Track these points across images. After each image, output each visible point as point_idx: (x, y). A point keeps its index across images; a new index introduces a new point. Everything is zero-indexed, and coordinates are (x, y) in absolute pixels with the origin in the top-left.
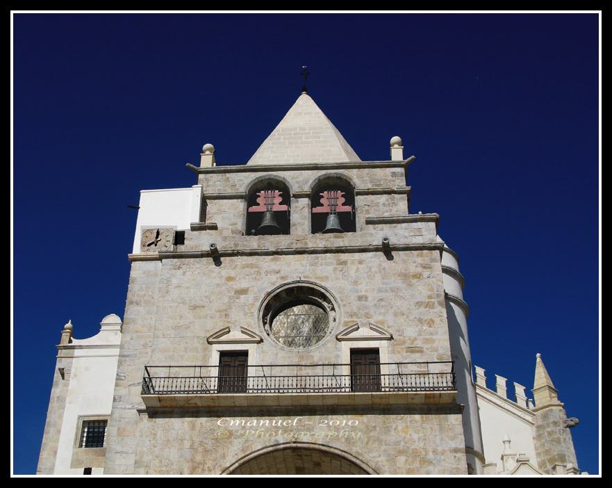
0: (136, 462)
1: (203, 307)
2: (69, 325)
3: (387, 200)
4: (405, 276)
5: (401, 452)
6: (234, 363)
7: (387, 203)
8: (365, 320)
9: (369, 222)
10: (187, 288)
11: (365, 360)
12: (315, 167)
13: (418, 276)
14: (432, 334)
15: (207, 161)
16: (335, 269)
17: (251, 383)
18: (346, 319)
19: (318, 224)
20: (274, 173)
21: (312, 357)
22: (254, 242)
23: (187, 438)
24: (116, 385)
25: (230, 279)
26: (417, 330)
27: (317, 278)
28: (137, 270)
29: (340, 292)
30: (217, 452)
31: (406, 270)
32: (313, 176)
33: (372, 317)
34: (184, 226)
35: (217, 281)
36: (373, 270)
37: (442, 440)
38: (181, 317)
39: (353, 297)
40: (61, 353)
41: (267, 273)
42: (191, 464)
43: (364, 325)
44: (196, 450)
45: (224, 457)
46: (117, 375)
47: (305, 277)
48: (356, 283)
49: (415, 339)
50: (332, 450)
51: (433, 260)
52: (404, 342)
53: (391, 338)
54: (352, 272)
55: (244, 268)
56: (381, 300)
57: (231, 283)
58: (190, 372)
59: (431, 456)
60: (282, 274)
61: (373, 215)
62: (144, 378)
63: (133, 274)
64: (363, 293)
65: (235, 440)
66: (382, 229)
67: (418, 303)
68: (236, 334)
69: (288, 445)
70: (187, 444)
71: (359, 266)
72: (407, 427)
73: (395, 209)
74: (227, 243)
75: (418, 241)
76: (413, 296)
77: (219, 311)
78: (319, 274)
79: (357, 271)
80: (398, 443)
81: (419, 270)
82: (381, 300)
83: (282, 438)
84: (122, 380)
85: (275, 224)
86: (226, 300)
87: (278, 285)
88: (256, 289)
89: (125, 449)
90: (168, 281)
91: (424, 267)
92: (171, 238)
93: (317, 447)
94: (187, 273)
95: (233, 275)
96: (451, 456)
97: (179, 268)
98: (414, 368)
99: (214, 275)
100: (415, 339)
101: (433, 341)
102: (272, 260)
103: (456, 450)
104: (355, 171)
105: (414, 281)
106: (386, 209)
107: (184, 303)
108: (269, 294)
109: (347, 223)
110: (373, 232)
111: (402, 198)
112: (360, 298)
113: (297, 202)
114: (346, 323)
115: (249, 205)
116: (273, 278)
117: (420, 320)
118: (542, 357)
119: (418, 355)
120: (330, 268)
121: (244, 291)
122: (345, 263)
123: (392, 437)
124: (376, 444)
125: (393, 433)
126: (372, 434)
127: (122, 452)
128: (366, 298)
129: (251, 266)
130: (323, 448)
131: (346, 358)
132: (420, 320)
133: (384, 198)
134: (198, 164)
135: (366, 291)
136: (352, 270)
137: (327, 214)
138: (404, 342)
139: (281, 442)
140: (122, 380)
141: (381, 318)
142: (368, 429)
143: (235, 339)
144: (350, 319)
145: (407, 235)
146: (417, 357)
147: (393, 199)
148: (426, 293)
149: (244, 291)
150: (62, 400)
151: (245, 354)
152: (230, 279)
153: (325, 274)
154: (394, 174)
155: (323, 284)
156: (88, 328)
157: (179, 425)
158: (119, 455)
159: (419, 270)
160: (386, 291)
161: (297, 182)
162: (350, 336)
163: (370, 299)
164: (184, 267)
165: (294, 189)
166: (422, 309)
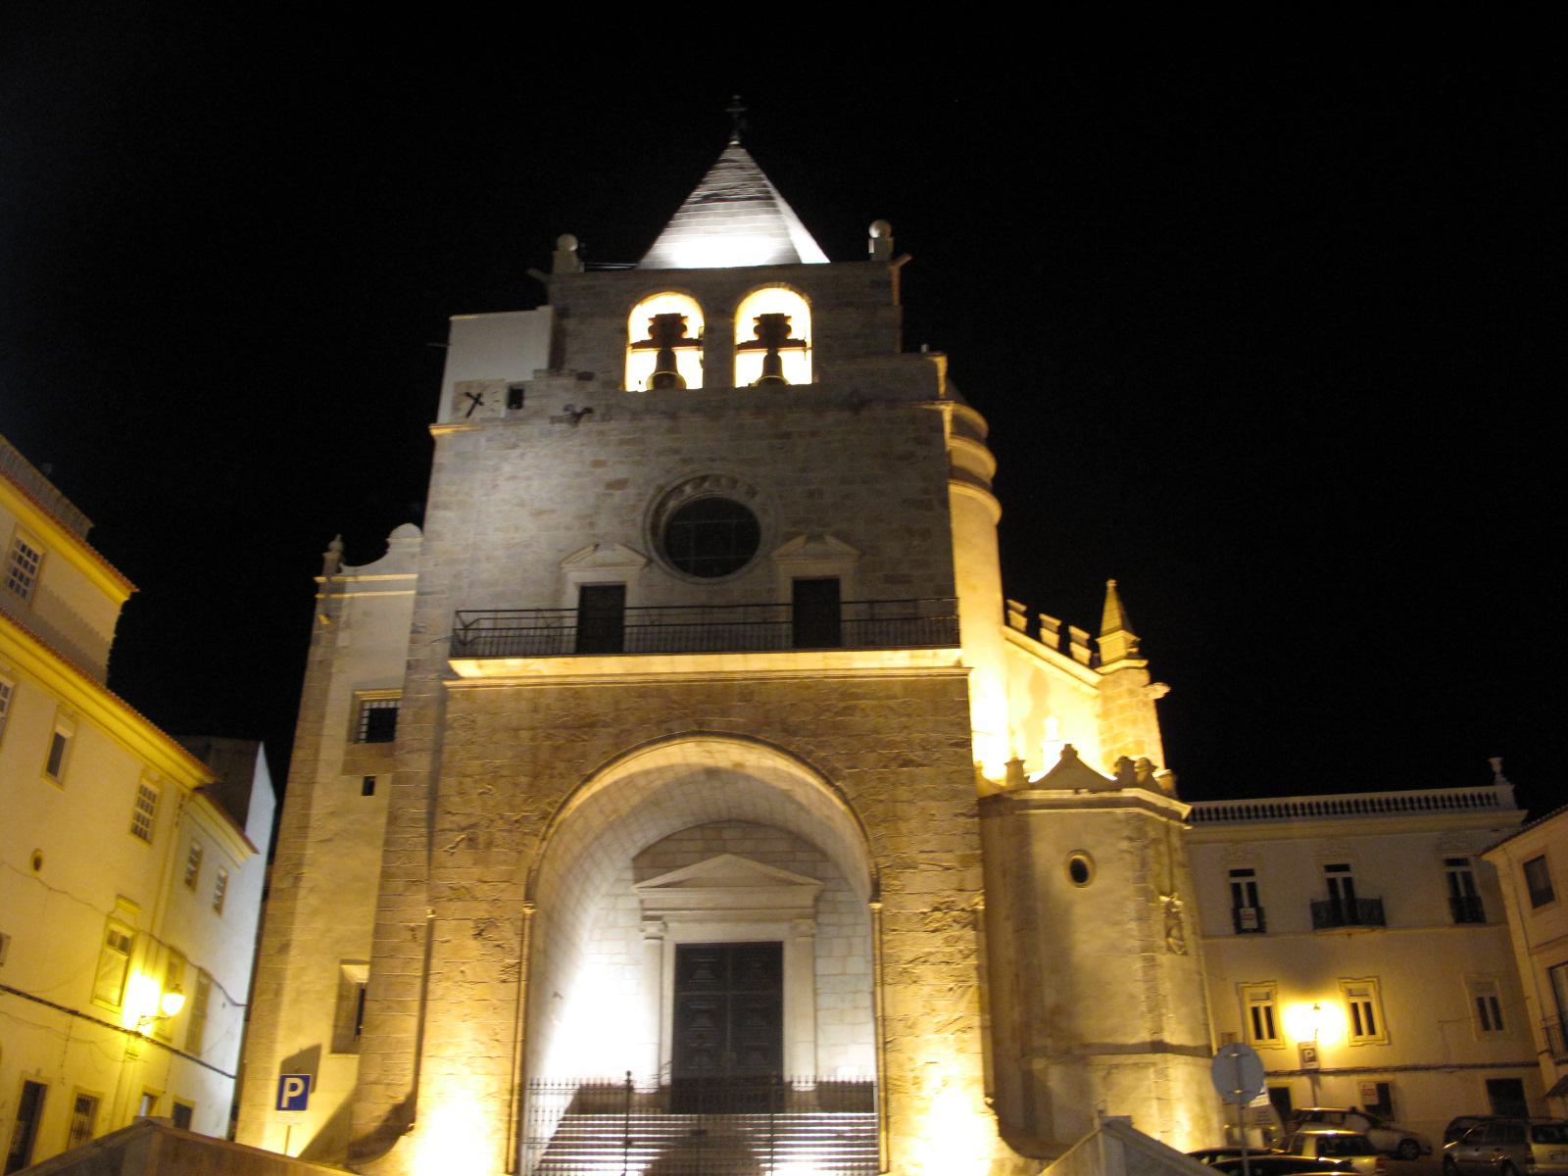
10: (528, 478)
24: (413, 641)
38: (517, 529)
45: (583, 756)
46: (413, 624)
57: (599, 471)
62: (454, 630)
65: (604, 730)
67: (904, 501)
70: (525, 735)
84: (420, 632)
92: (502, 396)
97: (514, 446)
98: (894, 609)
107: (521, 504)
112: (811, 494)
118: (1119, 590)
131: (786, 594)
140: (420, 632)
144: (793, 530)
150: (326, 664)
156: (368, 549)
164: (522, 444)
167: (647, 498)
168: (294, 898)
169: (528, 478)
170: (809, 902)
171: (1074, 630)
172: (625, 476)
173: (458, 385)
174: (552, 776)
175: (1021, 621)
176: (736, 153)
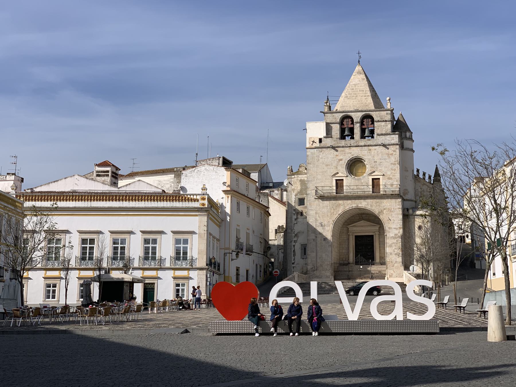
0: (316, 213)
3: (384, 124)
4: (388, 154)
5: (384, 209)
6: (339, 183)
9: (378, 135)
10: (324, 159)
11: (375, 182)
12: (362, 111)
13: (392, 154)
16: (368, 152)
19: (363, 137)
20: (348, 113)
21: (361, 181)
22: (343, 143)
23: (328, 205)
25: (337, 155)
26: (391, 172)
27: (362, 155)
32: (360, 115)
33: (378, 168)
34: (322, 137)
35: (333, 156)
36: (379, 152)
37: (395, 205)
39: (373, 161)
42: (330, 213)
44: (331, 209)
47: (359, 155)
48: (373, 157)
49: (390, 175)
51: (396, 149)
53: (384, 175)
54: (373, 153)
57: (337, 157)
58: (328, 188)
60: (352, 154)
61: (380, 133)
63: (308, 154)
64: (376, 160)
66: (382, 138)
70: (329, 208)
73: (387, 127)
74: (335, 142)
75: (393, 142)
76: (390, 161)
78: (363, 154)
79: (374, 153)
80: (384, 206)
81: (392, 152)
82: (381, 162)
83: (354, 206)
85: (349, 134)
86: (336, 163)
88: (344, 159)
89: (312, 209)
90: (319, 156)
91: (394, 151)
92: (318, 141)
96: (398, 210)
97: (321, 152)
99: (332, 154)
100: (390, 175)
101: (395, 176)
102: (349, 149)
103: (399, 208)
104: (375, 112)
105: (391, 156)
106: (384, 127)
107: (323, 164)
108: (348, 161)
110: (379, 138)
111: (389, 123)
112: (375, 162)
113: (356, 125)
114: (371, 170)
116: (350, 155)
119: (391, 180)
120: (366, 152)
121: (341, 160)
122: (370, 150)
123: (383, 205)
125: (383, 203)
126: (377, 204)
127: (311, 210)
128: (377, 162)
129: (343, 151)
130: (365, 208)
133: (383, 123)
136: (372, 152)
137: (365, 129)
138: (387, 176)
141: (381, 168)
142: (376, 203)
145: (389, 139)
146: (391, 181)
148: (394, 160)
149: (341, 160)
151: (343, 180)
152: (337, 155)
153: (365, 154)
157: (327, 203)
159: (392, 152)
160: (382, 160)
161: (356, 117)
163: (378, 162)
166: (393, 166)
168: (292, 233)
169: (324, 159)
170: (378, 229)
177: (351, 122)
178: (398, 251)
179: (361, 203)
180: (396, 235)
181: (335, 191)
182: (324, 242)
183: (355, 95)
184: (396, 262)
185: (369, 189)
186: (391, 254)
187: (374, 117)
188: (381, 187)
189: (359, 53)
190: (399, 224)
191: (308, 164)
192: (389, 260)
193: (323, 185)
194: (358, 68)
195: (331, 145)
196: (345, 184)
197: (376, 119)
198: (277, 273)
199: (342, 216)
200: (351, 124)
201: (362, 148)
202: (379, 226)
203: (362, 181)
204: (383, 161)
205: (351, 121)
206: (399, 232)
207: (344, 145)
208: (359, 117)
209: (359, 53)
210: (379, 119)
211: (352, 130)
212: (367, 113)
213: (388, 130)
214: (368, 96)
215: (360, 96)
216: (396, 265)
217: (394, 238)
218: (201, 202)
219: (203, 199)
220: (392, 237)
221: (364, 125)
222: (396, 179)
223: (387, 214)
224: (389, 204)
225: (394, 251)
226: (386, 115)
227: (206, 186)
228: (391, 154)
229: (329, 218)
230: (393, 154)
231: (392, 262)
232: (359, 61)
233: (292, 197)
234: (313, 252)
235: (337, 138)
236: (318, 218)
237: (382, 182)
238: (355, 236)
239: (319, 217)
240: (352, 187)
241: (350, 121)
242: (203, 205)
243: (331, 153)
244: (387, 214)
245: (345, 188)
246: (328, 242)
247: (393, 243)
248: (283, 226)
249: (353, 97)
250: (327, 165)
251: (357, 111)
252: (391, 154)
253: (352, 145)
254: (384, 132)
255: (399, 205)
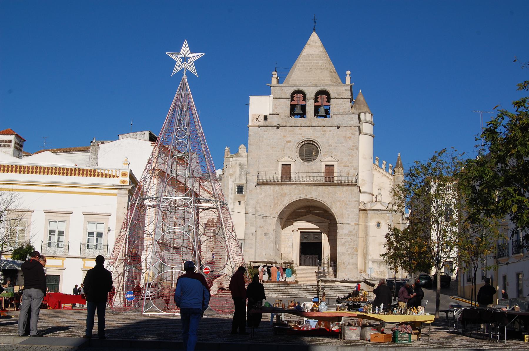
1: (275, 147)
2: (227, 148)
3: (342, 102)
4: (345, 137)
5: (339, 201)
6: (286, 168)
7: (342, 103)
8: (330, 154)
13: (350, 138)
14: (352, 160)
15: (274, 81)
16: (321, 134)
17: (292, 178)
18: (324, 154)
25: (284, 136)
27: (315, 137)
28: (251, 131)
29: (322, 143)
30: (281, 200)
31: (346, 135)
32: (315, 90)
40: (226, 159)
41: (297, 134)
43: (330, 156)
47: (310, 137)
48: (328, 140)
49: (347, 162)
50: (317, 200)
51: (356, 131)
52: (343, 162)
55: (289, 132)
56: (336, 146)
58: (272, 174)
59: (348, 202)
63: (250, 133)
64: (330, 144)
68: (286, 158)
69: (304, 198)
70: (272, 197)
71: (330, 133)
72: (341, 193)
75: (351, 123)
77: (281, 149)
81: (351, 135)
82: (336, 146)
83: (302, 196)
87: (301, 139)
92: (263, 118)
93: (313, 199)
94: (269, 134)
95: (285, 135)
97: (266, 131)
100: (347, 162)
101: (352, 163)
102: (300, 129)
105: (348, 139)
106: (342, 106)
107: (268, 145)
109: (327, 113)
111: (348, 101)
112: (329, 146)
115: (291, 101)
116: (300, 136)
117: (349, 155)
119: (347, 168)
120: (319, 133)
121: (289, 142)
122: (324, 131)
124: (331, 198)
125: (337, 195)
126: (330, 195)
127: (251, 199)
129: (292, 131)
132: (349, 155)
134: (271, 83)
135: (331, 143)
138: (343, 162)
139: (302, 197)
141: (336, 153)
143: (286, 160)
147: (344, 101)
151: (290, 165)
152: (284, 136)
154: (346, 90)
155: (317, 140)
156: (235, 152)
158: (250, 200)
159: (351, 135)
160: (338, 143)
161: (309, 92)
162: (325, 160)
163: (332, 146)
165: (308, 96)
166: (350, 151)
167: (295, 145)
169: (269, 139)
171: (390, 165)
172: (290, 140)
173: (252, 115)
174: (277, 205)
175: (377, 163)
176: (314, 37)
177: (303, 99)
178: (352, 250)
179: (310, 193)
180: (350, 232)
181: (280, 178)
182: (264, 238)
183: (309, 68)
184: (349, 263)
185: (322, 178)
186: (344, 254)
187: (331, 93)
188: (336, 175)
189: (314, 19)
190: (354, 220)
191: (250, 145)
192: (341, 261)
193: (266, 169)
194: (314, 37)
195: (279, 124)
196: (292, 169)
197: (332, 95)
198: (209, 271)
199: (287, 207)
200: (303, 101)
201: (315, 129)
202: (329, 221)
203: (313, 168)
204: (339, 144)
205: (302, 97)
206: (354, 229)
207: (293, 124)
208: (313, 92)
209: (314, 19)
210: (336, 96)
211: (304, 108)
212: (322, 88)
213: (346, 109)
214: (323, 69)
215: (314, 68)
216: (348, 267)
217: (348, 235)
218: (122, 178)
219: (124, 175)
220: (346, 234)
221: (318, 102)
222: (353, 166)
223: (341, 207)
224: (344, 196)
225: (348, 251)
226: (344, 91)
227: (129, 160)
228: (349, 138)
229: (272, 209)
230: (351, 137)
231: (344, 263)
232: (314, 28)
233: (228, 183)
234: (251, 248)
235: (285, 116)
236: (259, 209)
237: (336, 170)
238: (301, 232)
239: (260, 207)
240: (301, 174)
241: (301, 97)
242: (124, 182)
243: (278, 133)
244: (341, 207)
245: (292, 174)
246: (269, 237)
247: (348, 241)
248: (213, 219)
249: (306, 69)
250: (273, 148)
251: (311, 85)
252: (349, 138)
253: (303, 125)
254: (341, 112)
255: (355, 197)
